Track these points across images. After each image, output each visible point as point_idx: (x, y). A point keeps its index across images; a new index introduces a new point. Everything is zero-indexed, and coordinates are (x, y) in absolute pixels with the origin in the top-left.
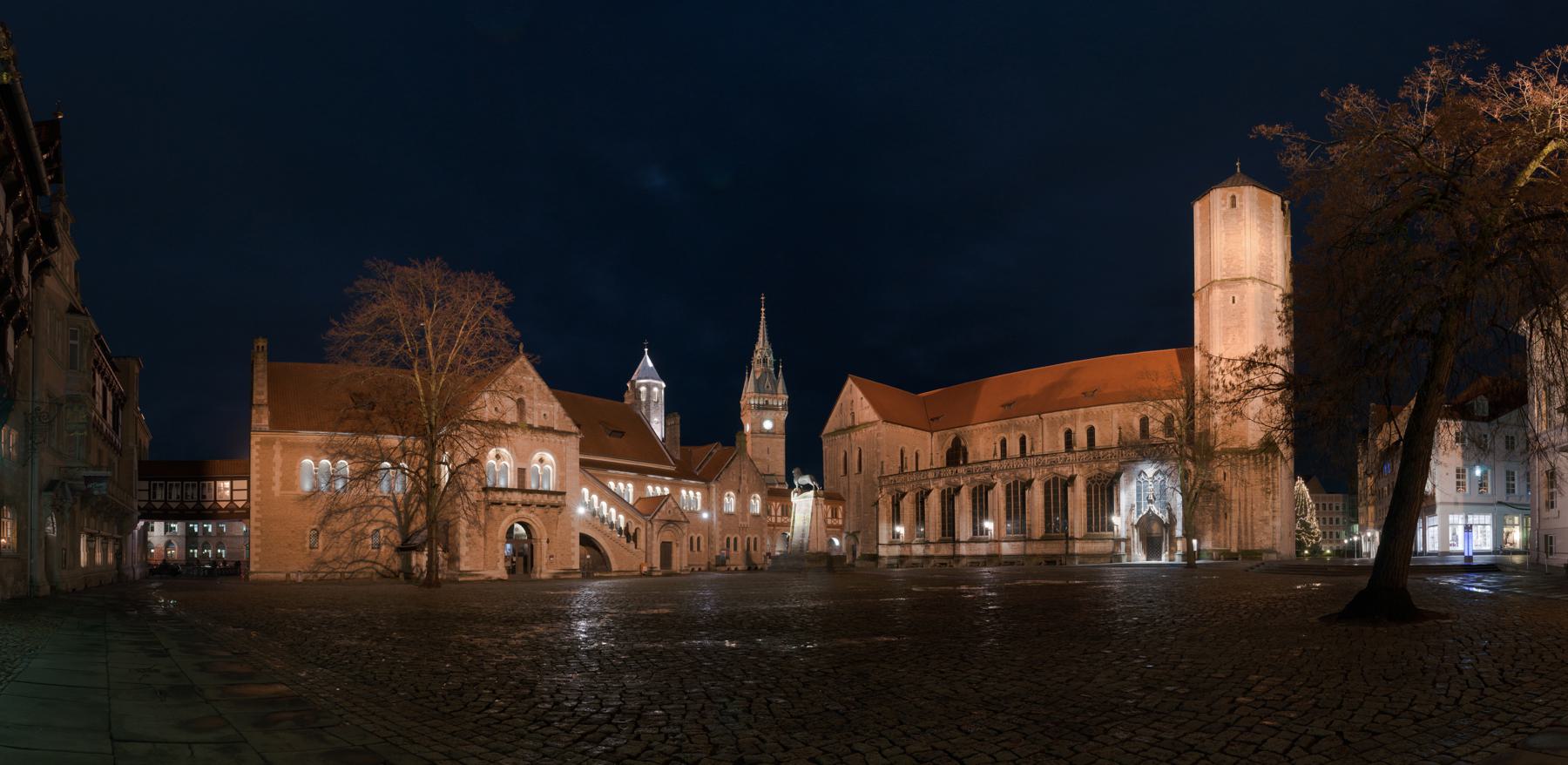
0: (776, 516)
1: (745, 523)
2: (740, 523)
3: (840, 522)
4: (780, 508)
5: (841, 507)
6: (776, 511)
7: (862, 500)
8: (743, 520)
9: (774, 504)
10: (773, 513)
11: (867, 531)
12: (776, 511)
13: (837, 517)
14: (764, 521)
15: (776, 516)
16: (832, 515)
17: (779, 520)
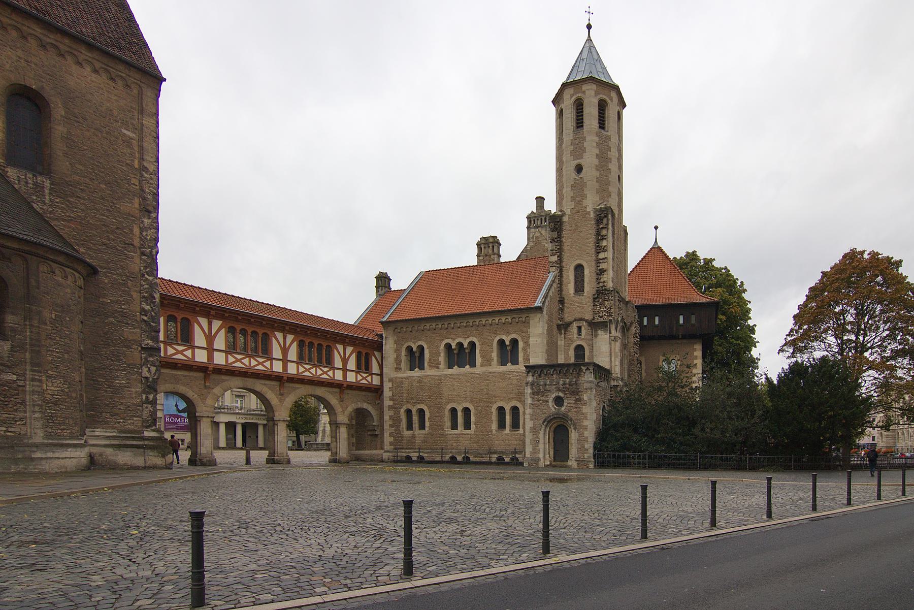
0: (210, 350)
3: (376, 381)
13: (368, 369)
16: (359, 366)
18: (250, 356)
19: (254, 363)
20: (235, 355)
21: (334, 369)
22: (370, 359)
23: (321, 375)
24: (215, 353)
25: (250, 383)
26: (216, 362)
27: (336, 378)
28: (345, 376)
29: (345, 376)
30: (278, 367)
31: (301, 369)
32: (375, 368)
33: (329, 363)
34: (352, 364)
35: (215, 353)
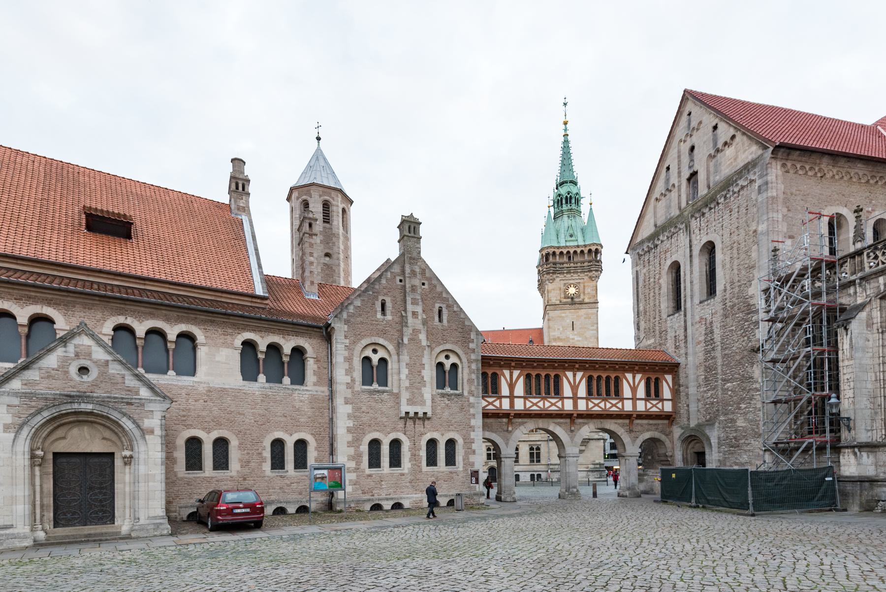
0: (512, 397)
1: (421, 411)
2: (405, 408)
4: (521, 380)
5: (669, 378)
6: (512, 387)
7: (718, 354)
8: (410, 402)
9: (507, 373)
10: (505, 390)
11: (733, 421)
12: (512, 387)
14: (471, 405)
15: (512, 397)
16: (648, 393)
17: (519, 405)
18: (543, 398)
19: (547, 404)
20: (530, 399)
21: (662, 400)
22: (660, 384)
23: (651, 408)
24: (516, 400)
25: (541, 423)
26: (516, 408)
27: (625, 410)
28: (634, 405)
29: (634, 405)
30: (568, 405)
31: (591, 405)
32: (667, 393)
33: (618, 393)
34: (641, 392)
35: (516, 400)
